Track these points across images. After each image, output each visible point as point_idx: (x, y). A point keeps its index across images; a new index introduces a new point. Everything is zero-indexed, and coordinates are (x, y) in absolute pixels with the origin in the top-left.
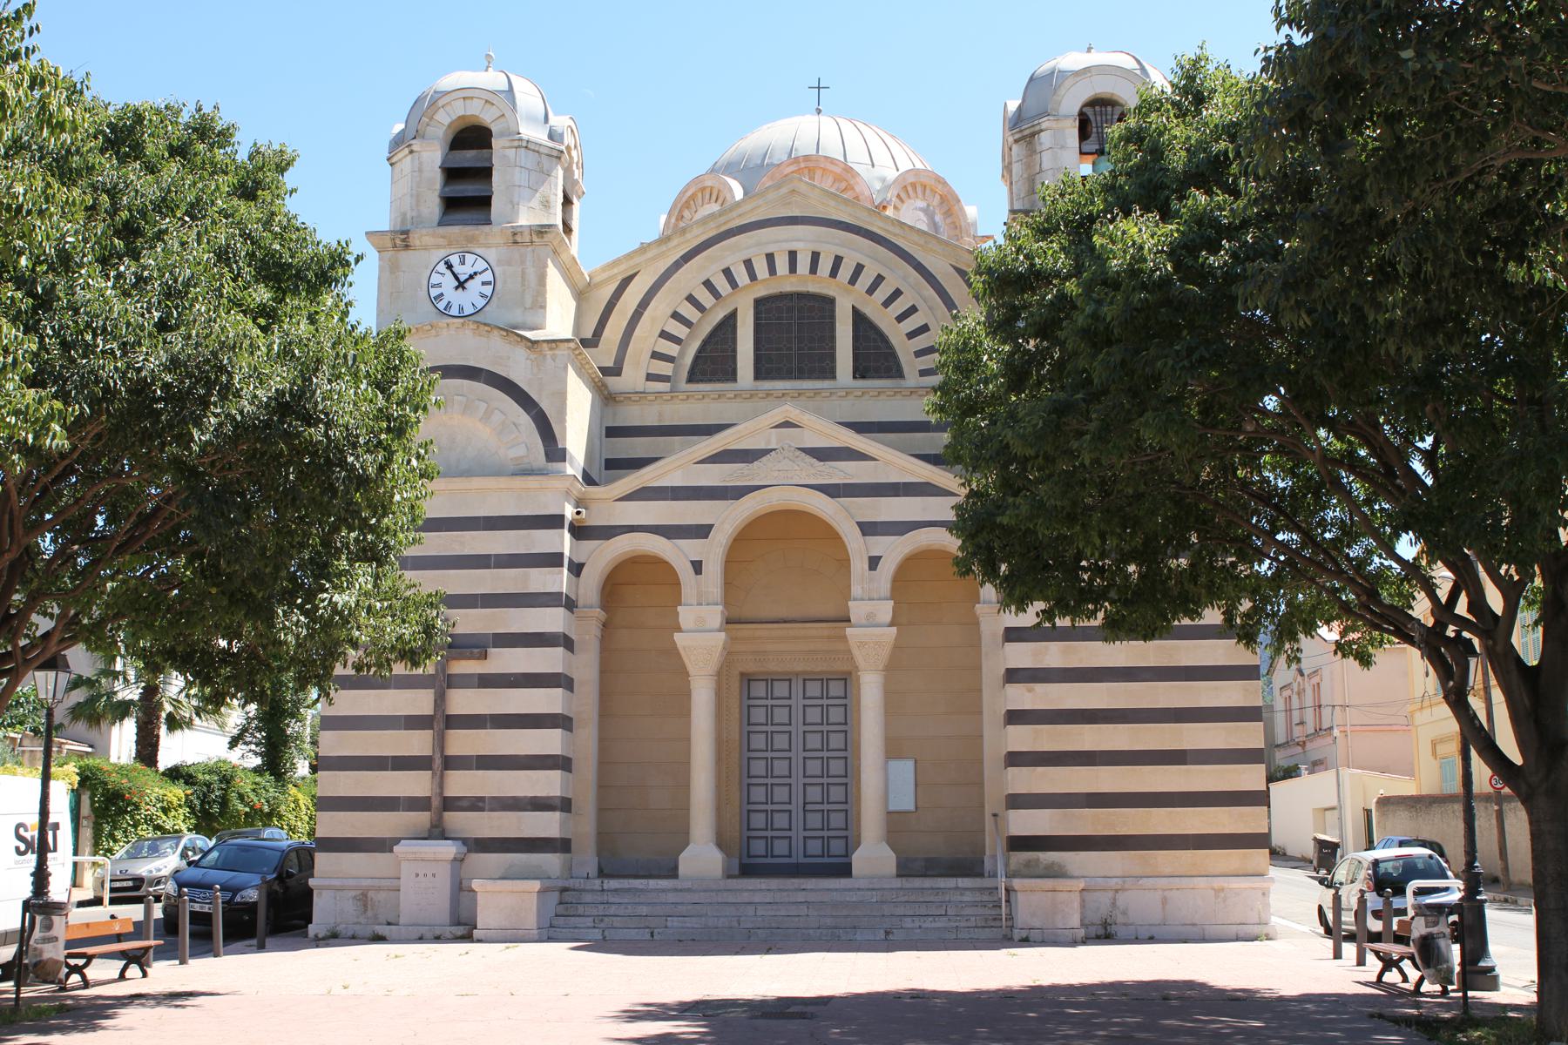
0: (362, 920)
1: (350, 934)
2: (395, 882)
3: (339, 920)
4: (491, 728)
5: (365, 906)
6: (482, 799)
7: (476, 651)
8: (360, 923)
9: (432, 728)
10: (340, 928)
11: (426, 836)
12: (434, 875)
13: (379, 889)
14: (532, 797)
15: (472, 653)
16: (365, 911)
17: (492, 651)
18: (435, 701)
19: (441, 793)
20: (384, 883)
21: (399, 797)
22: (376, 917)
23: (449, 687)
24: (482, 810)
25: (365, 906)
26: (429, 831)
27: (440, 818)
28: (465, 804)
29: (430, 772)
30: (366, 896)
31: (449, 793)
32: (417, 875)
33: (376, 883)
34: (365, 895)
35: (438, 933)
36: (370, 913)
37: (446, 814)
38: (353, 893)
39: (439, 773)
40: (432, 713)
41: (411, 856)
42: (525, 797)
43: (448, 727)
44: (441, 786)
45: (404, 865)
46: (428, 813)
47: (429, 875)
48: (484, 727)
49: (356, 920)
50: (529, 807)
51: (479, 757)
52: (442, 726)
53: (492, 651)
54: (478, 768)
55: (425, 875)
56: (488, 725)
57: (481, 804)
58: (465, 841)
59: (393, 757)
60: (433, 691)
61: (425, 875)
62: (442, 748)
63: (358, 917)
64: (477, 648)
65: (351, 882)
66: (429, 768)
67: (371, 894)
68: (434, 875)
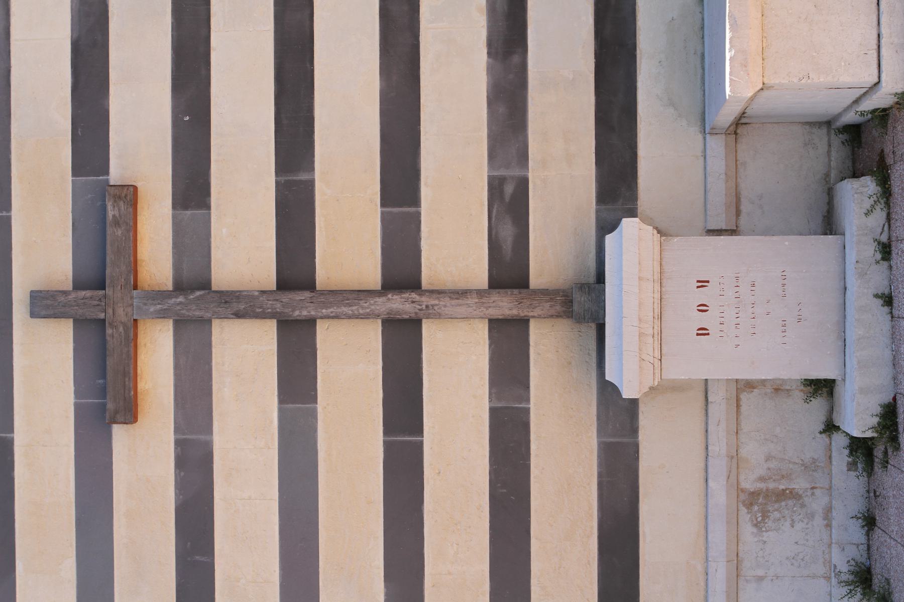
0: (817, 504)
1: (857, 533)
2: (718, 397)
3: (821, 570)
4: (312, 169)
5: (781, 495)
6: (495, 187)
7: (111, 212)
8: (828, 511)
9: (311, 323)
10: (841, 561)
11: (591, 332)
12: (702, 284)
13: (735, 459)
14: (489, 54)
15: (116, 223)
16: (793, 495)
17: (116, 174)
18: (238, 315)
19: (480, 293)
20: (719, 446)
21: (493, 412)
22: (809, 467)
23: (205, 284)
24: (523, 185)
25: (781, 495)
26: (580, 319)
27: (546, 294)
28: (507, 232)
29: (428, 330)
30: (754, 494)
31: (479, 275)
32: (703, 332)
33: (718, 466)
34: (751, 499)
35: (870, 251)
36: (800, 484)
37: (535, 281)
38: (748, 530)
39: (426, 300)
40: (271, 326)
41: (651, 349)
42: (490, 70)
43: (309, 285)
44: (461, 294)
45: (675, 371)
46: (533, 324)
47: (702, 296)
48: (310, 186)
49: (819, 521)
50: (516, 59)
51: (387, 199)
52: (307, 294)
53: (116, 174)
54: (414, 199)
55: (703, 308)
56: (303, 177)
57: (509, 189)
58: (606, 227)
59: (386, 432)
60: (216, 325)
61: (703, 308)
62: (370, 293)
63: (811, 516)
64: (104, 208)
65: (719, 534)
66: (415, 324)
67: (749, 483)
68: (702, 284)
